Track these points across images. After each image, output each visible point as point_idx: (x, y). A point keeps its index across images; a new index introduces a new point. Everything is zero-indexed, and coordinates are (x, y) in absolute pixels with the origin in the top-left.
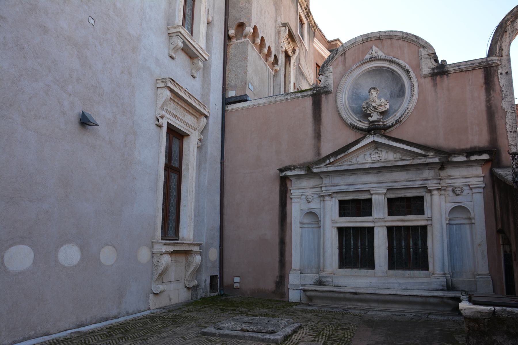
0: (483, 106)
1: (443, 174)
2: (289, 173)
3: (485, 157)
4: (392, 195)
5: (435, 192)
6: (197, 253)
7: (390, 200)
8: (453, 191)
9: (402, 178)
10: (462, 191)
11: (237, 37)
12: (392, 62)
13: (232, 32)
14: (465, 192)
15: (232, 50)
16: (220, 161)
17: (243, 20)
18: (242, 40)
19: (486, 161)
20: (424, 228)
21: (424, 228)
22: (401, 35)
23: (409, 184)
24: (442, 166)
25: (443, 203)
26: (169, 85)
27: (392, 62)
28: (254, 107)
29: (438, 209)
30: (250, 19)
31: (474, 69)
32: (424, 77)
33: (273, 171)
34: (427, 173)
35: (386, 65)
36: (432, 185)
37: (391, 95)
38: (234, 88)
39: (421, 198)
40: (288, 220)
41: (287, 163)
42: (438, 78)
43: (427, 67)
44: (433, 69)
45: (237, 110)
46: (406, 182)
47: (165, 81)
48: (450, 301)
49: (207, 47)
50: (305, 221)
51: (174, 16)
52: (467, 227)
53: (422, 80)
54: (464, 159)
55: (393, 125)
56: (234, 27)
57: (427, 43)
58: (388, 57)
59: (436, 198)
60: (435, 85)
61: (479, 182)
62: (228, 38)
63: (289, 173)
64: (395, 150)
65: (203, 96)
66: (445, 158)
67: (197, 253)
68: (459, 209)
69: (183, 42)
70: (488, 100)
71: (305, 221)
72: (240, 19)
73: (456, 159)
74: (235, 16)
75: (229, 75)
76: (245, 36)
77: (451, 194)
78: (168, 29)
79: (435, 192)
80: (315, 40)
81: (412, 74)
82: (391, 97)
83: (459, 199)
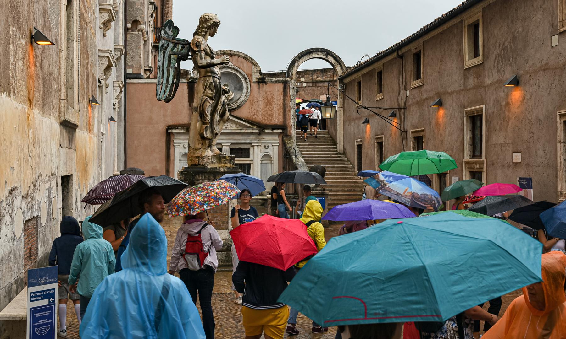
0: (281, 103)
1: (260, 137)
2: (174, 131)
3: (280, 131)
4: (233, 147)
5: (256, 147)
7: (232, 149)
8: (264, 146)
9: (239, 138)
10: (268, 147)
12: (237, 71)
13: (129, 26)
14: (270, 147)
17: (138, 18)
18: (137, 32)
19: (281, 133)
20: (249, 165)
21: (249, 165)
22: (243, 55)
23: (243, 142)
24: (259, 134)
25: (259, 152)
27: (237, 71)
29: (256, 155)
31: (279, 83)
32: (254, 82)
33: (162, 128)
34: (252, 137)
35: (234, 72)
36: (254, 143)
37: (235, 88)
38: (132, 67)
39: (248, 149)
40: (172, 158)
41: (171, 123)
42: (261, 84)
43: (256, 77)
44: (259, 79)
45: (134, 83)
46: (242, 141)
48: (260, 201)
50: (182, 159)
52: (270, 164)
53: (252, 84)
54: (270, 131)
55: (236, 108)
57: (256, 63)
58: (235, 67)
59: (256, 150)
60: (259, 88)
61: (277, 142)
62: (126, 30)
64: (236, 123)
66: (261, 128)
68: (266, 156)
70: (284, 101)
71: (182, 159)
72: (136, 17)
73: (267, 131)
76: (139, 30)
77: (263, 147)
79: (256, 147)
81: (248, 80)
82: (235, 89)
83: (267, 150)
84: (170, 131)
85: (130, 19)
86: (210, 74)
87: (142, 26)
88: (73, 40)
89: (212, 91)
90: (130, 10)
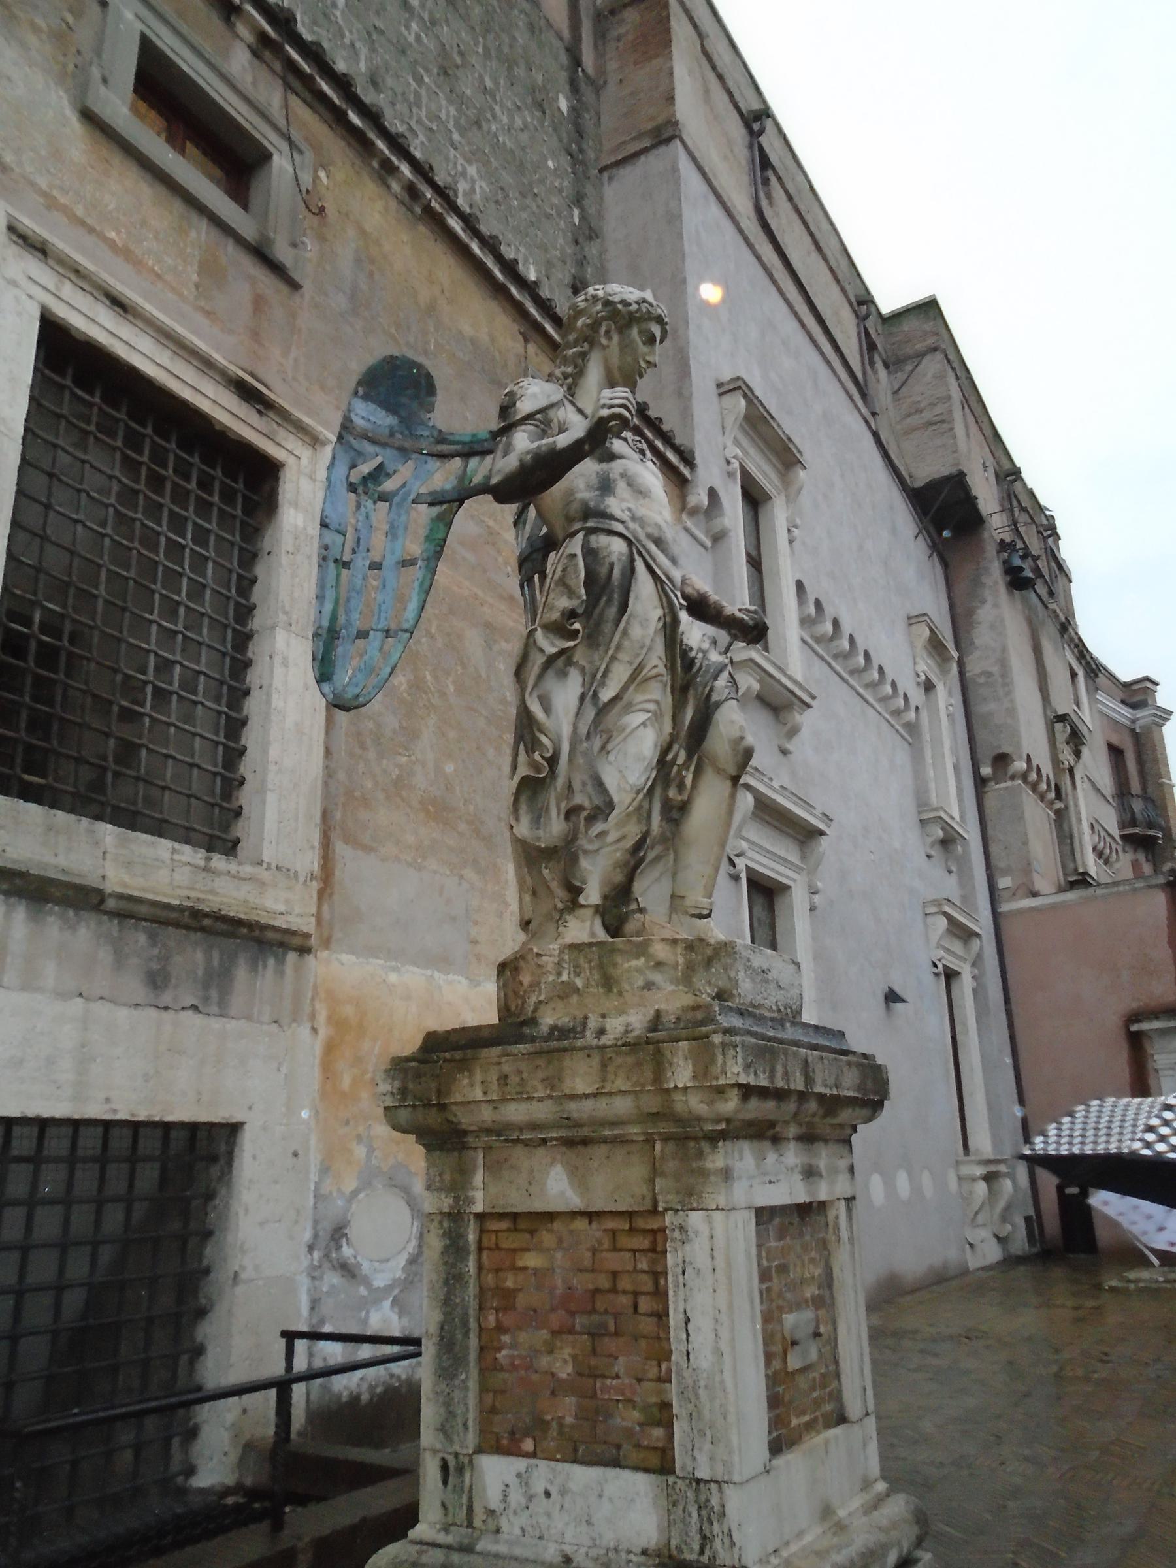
6: (1006, 1175)
11: (996, 778)
13: (986, 771)
15: (990, 801)
16: (1003, 1008)
17: (1005, 749)
26: (947, 909)
28: (1053, 907)
30: (1018, 745)
38: (1006, 872)
47: (937, 903)
49: (961, 817)
51: (927, 791)
56: (989, 762)
62: (981, 783)
63: (1145, 1026)
65: (964, 898)
67: (1006, 1175)
69: (942, 829)
74: (989, 744)
75: (994, 849)
76: (1013, 778)
78: (919, 813)
80: (1100, 696)
84: (1135, 1028)
85: (986, 755)
86: (578, 525)
87: (1020, 765)
88: (273, 628)
89: (571, 593)
90: (981, 735)
